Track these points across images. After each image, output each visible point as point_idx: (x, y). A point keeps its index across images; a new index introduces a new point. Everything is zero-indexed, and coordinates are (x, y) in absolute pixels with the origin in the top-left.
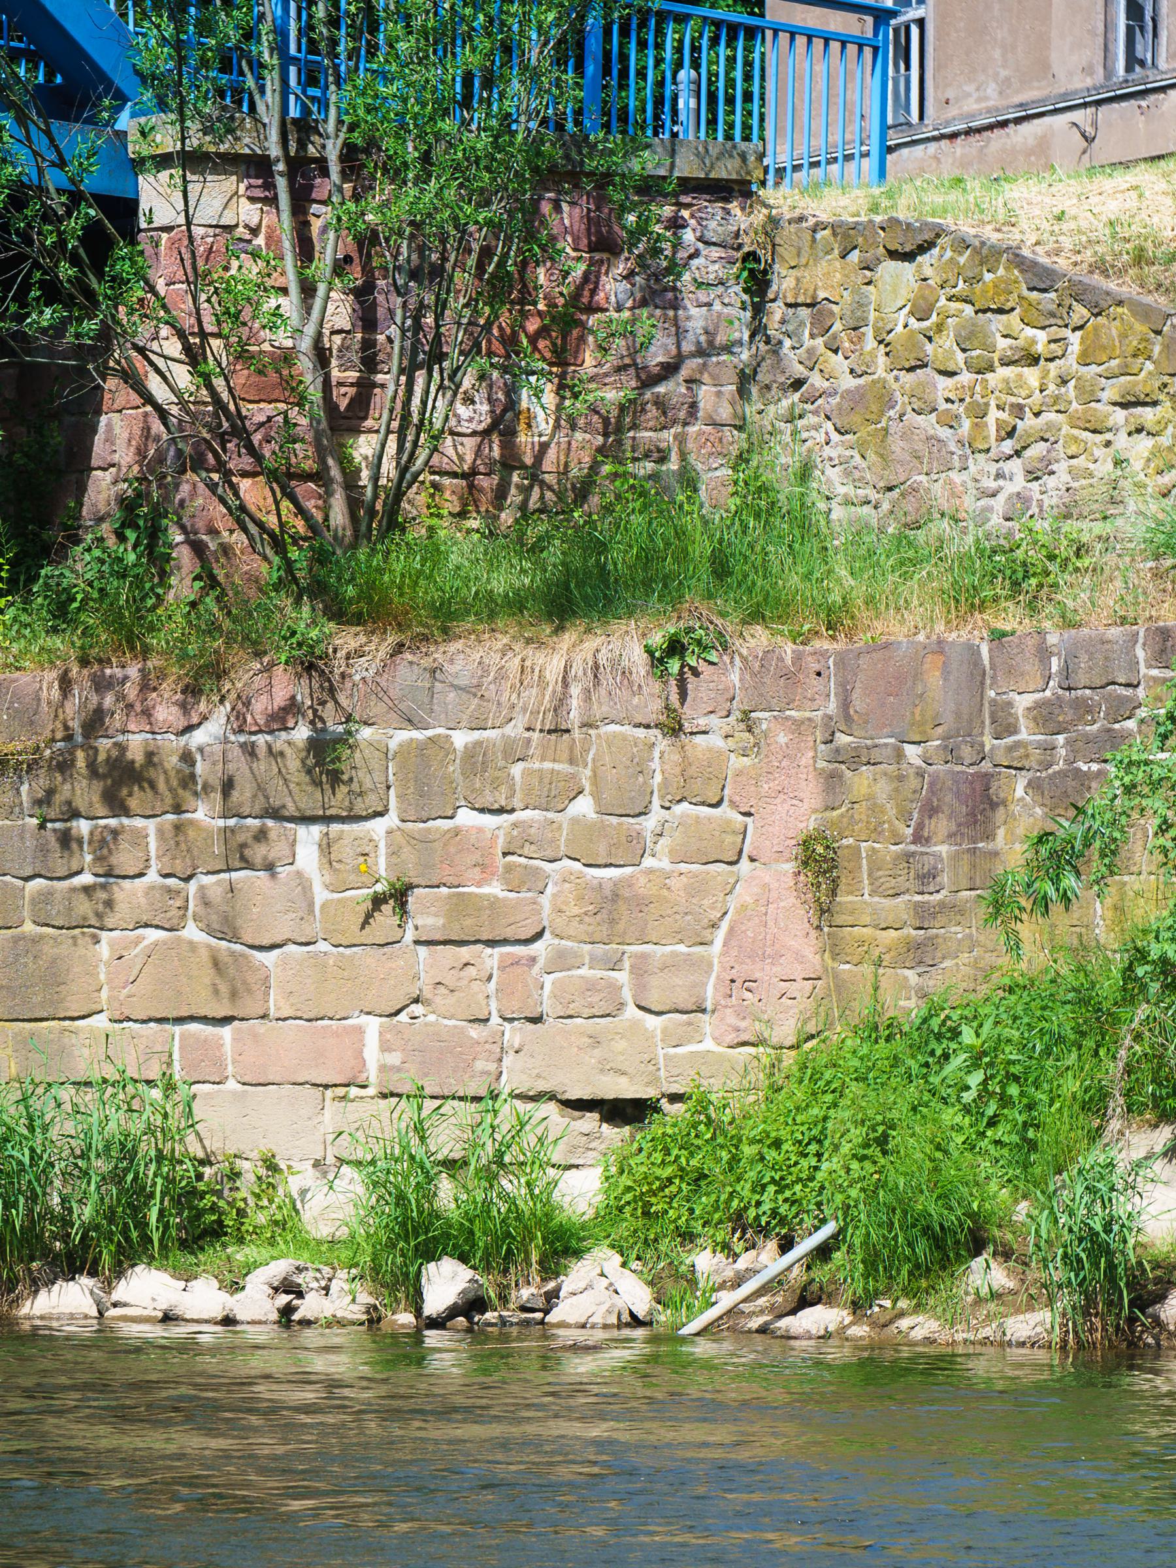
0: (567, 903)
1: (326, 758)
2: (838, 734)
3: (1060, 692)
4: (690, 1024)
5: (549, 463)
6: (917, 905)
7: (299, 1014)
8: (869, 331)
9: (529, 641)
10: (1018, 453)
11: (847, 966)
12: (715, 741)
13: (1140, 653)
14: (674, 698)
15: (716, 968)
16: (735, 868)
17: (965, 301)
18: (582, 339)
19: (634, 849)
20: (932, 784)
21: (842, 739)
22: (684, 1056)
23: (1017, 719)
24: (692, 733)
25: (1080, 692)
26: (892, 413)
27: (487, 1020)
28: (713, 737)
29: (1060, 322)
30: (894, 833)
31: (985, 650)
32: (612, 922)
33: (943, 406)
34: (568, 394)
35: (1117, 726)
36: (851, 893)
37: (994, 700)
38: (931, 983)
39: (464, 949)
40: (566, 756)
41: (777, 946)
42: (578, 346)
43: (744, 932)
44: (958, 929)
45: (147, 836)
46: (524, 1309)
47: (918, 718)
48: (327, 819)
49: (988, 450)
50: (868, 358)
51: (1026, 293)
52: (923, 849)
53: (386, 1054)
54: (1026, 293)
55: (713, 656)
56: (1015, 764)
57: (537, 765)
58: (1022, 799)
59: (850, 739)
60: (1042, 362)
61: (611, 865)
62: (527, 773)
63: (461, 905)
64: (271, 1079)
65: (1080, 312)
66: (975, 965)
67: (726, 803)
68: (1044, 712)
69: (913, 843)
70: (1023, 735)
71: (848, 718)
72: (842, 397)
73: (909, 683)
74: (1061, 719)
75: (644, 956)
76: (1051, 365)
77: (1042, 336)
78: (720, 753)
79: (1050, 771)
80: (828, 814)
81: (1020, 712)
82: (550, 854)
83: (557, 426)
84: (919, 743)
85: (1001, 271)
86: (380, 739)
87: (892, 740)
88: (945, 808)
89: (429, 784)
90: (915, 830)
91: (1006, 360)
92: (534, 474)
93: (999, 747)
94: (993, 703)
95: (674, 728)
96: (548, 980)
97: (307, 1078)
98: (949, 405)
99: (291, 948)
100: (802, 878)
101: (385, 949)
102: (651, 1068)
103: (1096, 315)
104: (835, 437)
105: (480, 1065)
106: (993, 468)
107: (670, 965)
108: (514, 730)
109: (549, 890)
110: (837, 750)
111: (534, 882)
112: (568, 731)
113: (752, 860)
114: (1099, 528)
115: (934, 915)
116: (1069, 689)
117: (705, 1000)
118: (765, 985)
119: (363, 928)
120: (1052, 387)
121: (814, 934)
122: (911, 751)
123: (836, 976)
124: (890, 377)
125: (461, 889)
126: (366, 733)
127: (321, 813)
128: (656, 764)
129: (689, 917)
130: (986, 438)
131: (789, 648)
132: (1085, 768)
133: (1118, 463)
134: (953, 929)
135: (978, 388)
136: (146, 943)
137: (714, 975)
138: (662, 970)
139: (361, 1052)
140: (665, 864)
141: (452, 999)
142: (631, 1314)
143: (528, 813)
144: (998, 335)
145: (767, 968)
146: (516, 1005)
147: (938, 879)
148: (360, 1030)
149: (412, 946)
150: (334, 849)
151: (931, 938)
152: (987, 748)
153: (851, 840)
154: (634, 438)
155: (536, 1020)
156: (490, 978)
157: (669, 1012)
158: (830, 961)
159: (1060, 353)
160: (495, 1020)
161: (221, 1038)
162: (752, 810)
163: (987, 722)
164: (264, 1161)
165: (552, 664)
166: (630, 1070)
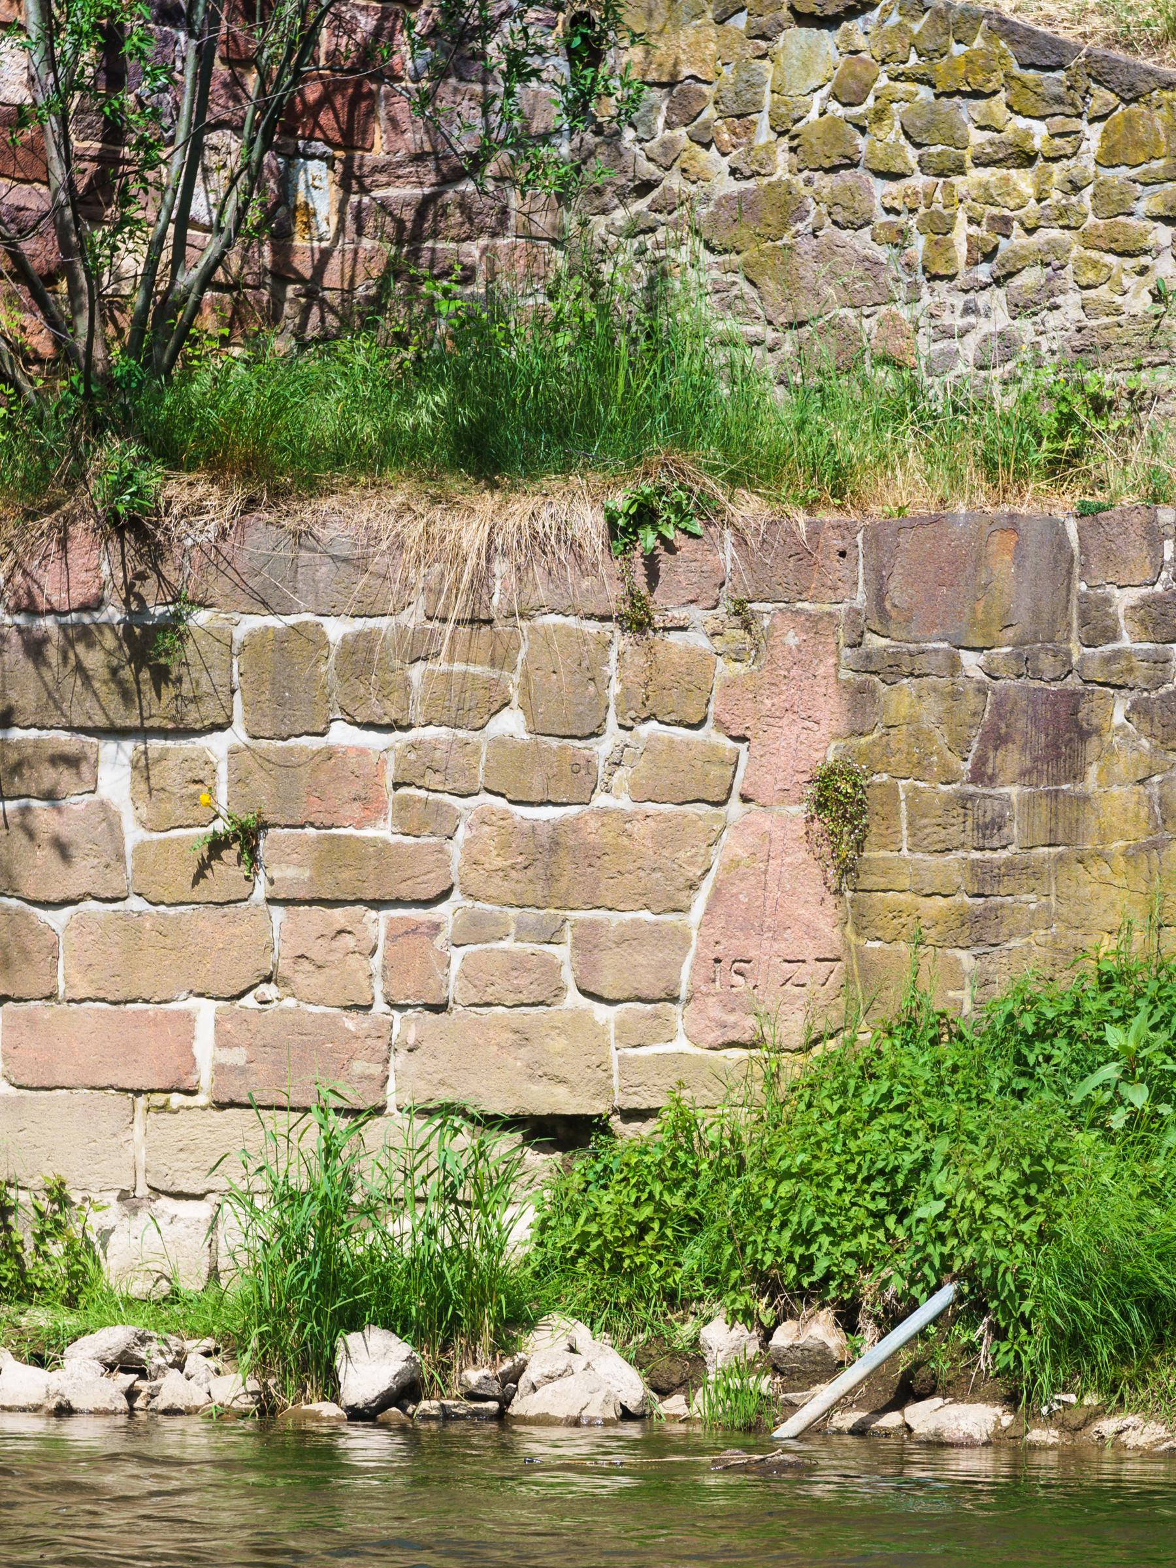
0: (486, 853)
1: (149, 649)
2: (868, 635)
4: (656, 1016)
5: (332, 277)
6: (975, 864)
7: (102, 994)
8: (763, 121)
9: (435, 500)
10: (998, 282)
11: (877, 944)
12: (697, 640)
14: (640, 580)
15: (694, 943)
16: (721, 811)
17: (920, 81)
18: (371, 112)
19: (580, 782)
20: (998, 705)
21: (875, 642)
22: (647, 1060)
23: (1118, 620)
24: (665, 629)
26: (800, 226)
27: (370, 1007)
28: (694, 634)
29: (1069, 110)
30: (946, 768)
31: (1072, 527)
32: (550, 879)
33: (882, 218)
34: (355, 187)
36: (884, 847)
37: (1085, 595)
38: (991, 968)
39: (338, 911)
40: (486, 655)
41: (781, 916)
42: (366, 123)
43: (735, 895)
47: (980, 616)
48: (142, 733)
49: (951, 278)
50: (762, 155)
51: (1016, 71)
52: (985, 791)
53: (225, 1050)
54: (1016, 71)
55: (697, 527)
56: (1114, 680)
58: (1121, 727)
59: (885, 642)
60: (1039, 162)
61: (549, 803)
62: (429, 677)
63: (335, 852)
65: (1101, 98)
66: (1054, 946)
67: (710, 723)
68: (1155, 613)
70: (1125, 642)
71: (883, 614)
72: (719, 205)
73: (970, 570)
75: (594, 925)
76: (1055, 167)
77: (1040, 129)
78: (704, 656)
79: (1162, 691)
80: (854, 741)
81: (1121, 612)
82: (462, 786)
83: (341, 229)
84: (980, 650)
85: (978, 42)
86: (225, 627)
87: (945, 645)
88: (1017, 737)
89: (288, 685)
90: (974, 765)
91: (984, 159)
92: (312, 290)
94: (1083, 598)
95: (638, 622)
96: (457, 955)
98: (892, 218)
99: (92, 905)
100: (817, 825)
101: (226, 909)
102: (601, 1074)
103: (1128, 102)
104: (706, 257)
105: (358, 1067)
106: (959, 301)
107: (629, 938)
108: (413, 618)
109: (462, 834)
110: (868, 657)
111: (439, 823)
112: (490, 621)
113: (745, 799)
114: (1128, 381)
115: (998, 879)
117: (678, 985)
118: (763, 967)
119: (195, 882)
120: (1056, 195)
121: (831, 900)
122: (970, 661)
123: (861, 955)
124: (798, 180)
125: (334, 831)
126: (201, 617)
127: (137, 723)
128: (612, 669)
129: (658, 875)
130: (950, 261)
131: (802, 518)
133: (1158, 297)
134: (1024, 897)
135: (938, 195)
138: (618, 944)
139: (190, 1046)
140: (624, 803)
141: (319, 979)
142: (623, 1407)
143: (431, 732)
144: (971, 126)
145: (766, 944)
146: (411, 986)
147: (1005, 830)
148: (188, 1018)
149: (264, 906)
152: (1075, 658)
153: (885, 777)
154: (433, 250)
155: (439, 1008)
156: (373, 952)
157: (628, 1000)
158: (853, 937)
159: (1069, 151)
160: (380, 1006)
162: (748, 734)
163: (1075, 624)
165: (470, 534)
166: (571, 1077)
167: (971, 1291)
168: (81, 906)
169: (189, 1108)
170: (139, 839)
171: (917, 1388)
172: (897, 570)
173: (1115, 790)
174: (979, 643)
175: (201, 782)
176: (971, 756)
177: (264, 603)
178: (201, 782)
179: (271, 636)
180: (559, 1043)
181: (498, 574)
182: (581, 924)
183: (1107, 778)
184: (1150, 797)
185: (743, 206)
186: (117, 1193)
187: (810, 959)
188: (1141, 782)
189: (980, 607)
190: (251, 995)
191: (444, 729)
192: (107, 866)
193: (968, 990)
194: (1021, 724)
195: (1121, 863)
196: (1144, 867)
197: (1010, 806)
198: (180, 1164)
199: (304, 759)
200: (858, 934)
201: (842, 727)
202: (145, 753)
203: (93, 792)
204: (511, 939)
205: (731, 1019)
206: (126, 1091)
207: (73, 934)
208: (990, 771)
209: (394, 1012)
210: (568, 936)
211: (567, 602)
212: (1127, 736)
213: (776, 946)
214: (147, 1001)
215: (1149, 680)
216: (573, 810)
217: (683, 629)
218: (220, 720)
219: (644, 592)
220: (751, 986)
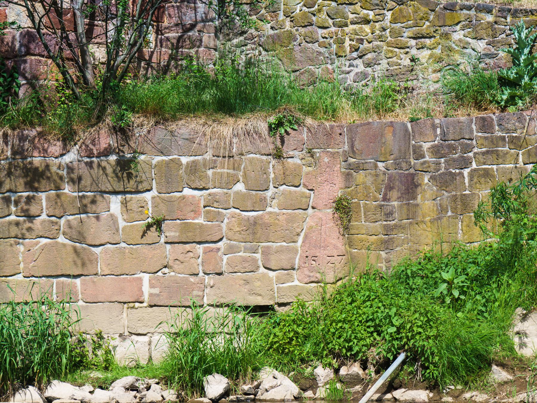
0: (234, 226)
1: (125, 166)
3: (441, 142)
4: (288, 274)
5: (154, 59)
6: (385, 225)
7: (113, 273)
8: (281, 13)
9: (214, 121)
10: (360, 57)
11: (356, 250)
12: (297, 161)
13: (474, 127)
14: (279, 143)
15: (299, 252)
16: (306, 212)
18: (164, 12)
19: (262, 204)
21: (352, 160)
22: (286, 288)
24: (288, 158)
25: (449, 142)
26: (295, 43)
27: (198, 274)
28: (295, 159)
29: (381, 8)
30: (375, 197)
31: (409, 125)
32: (254, 233)
33: (322, 40)
34: (160, 33)
35: (465, 155)
36: (357, 221)
37: (414, 145)
38: (391, 257)
39: (187, 245)
42: (162, 15)
43: (312, 237)
44: (402, 235)
45: (41, 200)
46: (246, 394)
47: (383, 152)
48: (124, 193)
50: (282, 23)
52: (387, 203)
53: (153, 289)
55: (296, 127)
56: (424, 170)
57: (219, 170)
58: (427, 184)
61: (253, 211)
62: (214, 174)
63: (187, 228)
64: (100, 300)
67: (302, 185)
68: (436, 150)
69: (383, 201)
70: (427, 158)
71: (354, 152)
72: (268, 37)
73: (379, 138)
74: (443, 152)
75: (268, 247)
76: (377, 24)
78: (299, 166)
79: (439, 173)
80: (346, 190)
81: (425, 150)
83: (156, 46)
84: (383, 162)
86: (149, 160)
87: (373, 160)
89: (169, 176)
90: (383, 196)
92: (149, 63)
93: (417, 163)
94: (414, 146)
95: (278, 156)
96: (225, 258)
97: (117, 300)
98: (325, 40)
99: (109, 246)
100: (336, 215)
101: (152, 246)
102: (271, 293)
103: (400, 5)
104: (263, 53)
105: (195, 293)
106: (348, 63)
107: (279, 251)
109: (226, 221)
110: (350, 165)
111: (219, 217)
113: (313, 208)
116: (445, 141)
117: (295, 265)
118: (321, 258)
119: (142, 237)
121: (341, 237)
123: (351, 254)
124: (294, 30)
125: (185, 221)
126: (142, 157)
128: (271, 170)
129: (287, 231)
132: (454, 171)
133: (413, 60)
134: (400, 235)
135: (339, 33)
136: (41, 244)
137: (299, 254)
138: (276, 253)
140: (276, 210)
141: (182, 266)
143: (215, 190)
144: (349, 13)
145: (322, 251)
146: (211, 268)
147: (394, 215)
148: (140, 279)
149: (164, 244)
150: (128, 204)
151: (391, 239)
152: (412, 164)
153: (356, 200)
154: (182, 52)
155: (220, 274)
156: (199, 258)
158: (348, 249)
160: (201, 274)
161: (76, 283)
162: (314, 188)
163: (412, 154)
164: (97, 335)
167: (411, 355)
168: (106, 246)
169: (141, 307)
170: (124, 225)
171: (395, 386)
172: (357, 139)
173: (426, 202)
174: (383, 160)
175: (143, 207)
176: (382, 193)
177: (162, 152)
178: (143, 207)
179: (164, 162)
180: (258, 284)
181: (235, 143)
182: (264, 247)
183: (424, 199)
184: (437, 204)
185: (275, 39)
186: (118, 335)
187: (336, 256)
188: (434, 200)
189: (383, 149)
190: (160, 272)
191: (219, 189)
192: (114, 234)
193: (384, 263)
194: (397, 183)
195: (429, 224)
196: (436, 225)
197: (395, 208)
198: (138, 325)
199: (176, 199)
200: (350, 248)
201: (342, 185)
202: (125, 199)
203: (109, 211)
204: (242, 252)
205: (312, 274)
206: (121, 302)
207: (103, 255)
208: (388, 198)
209: (206, 276)
210: (260, 251)
211: (257, 150)
212: (429, 186)
213: (325, 252)
214: (127, 275)
215: (435, 169)
216: (261, 212)
217: (292, 157)
218: (149, 188)
219: (280, 147)
220: (317, 264)
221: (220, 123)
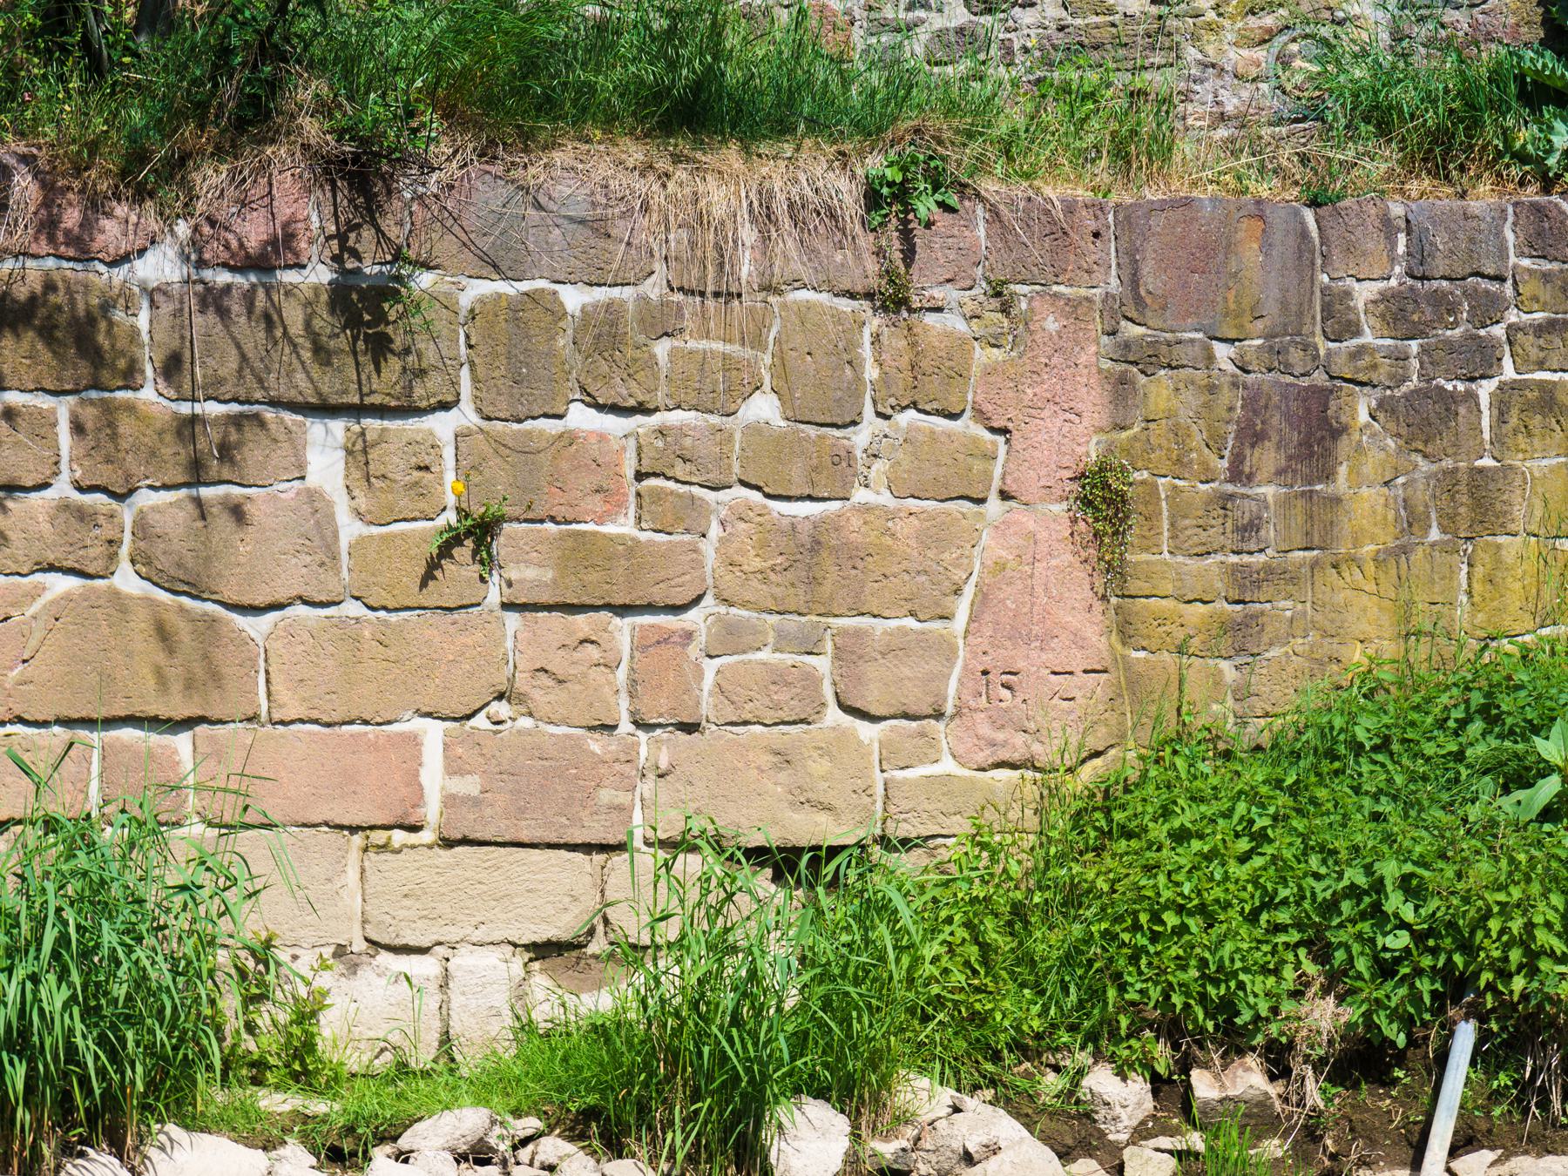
3: (1410, 281)
6: (1235, 569)
7: (315, 715)
9: (677, 159)
11: (1142, 654)
15: (961, 653)
19: (835, 474)
23: (1358, 315)
25: (1435, 284)
27: (615, 727)
28: (950, 318)
30: (1206, 467)
32: (813, 581)
35: (1482, 332)
37: (1328, 288)
39: (580, 619)
43: (1002, 601)
44: (1289, 604)
47: (1232, 306)
52: (1243, 490)
53: (456, 779)
56: (1362, 377)
57: (692, 344)
58: (1367, 426)
61: (810, 498)
62: (673, 354)
63: (582, 552)
68: (1394, 308)
69: (1231, 481)
70: (1368, 338)
74: (1415, 317)
75: (858, 634)
79: (1404, 389)
81: (1361, 306)
82: (714, 477)
84: (1231, 341)
86: (453, 289)
87: (1200, 335)
90: (1232, 463)
93: (1337, 352)
94: (1325, 290)
95: (893, 300)
97: (328, 816)
99: (300, 610)
101: (456, 616)
107: (896, 648)
108: (653, 289)
109: (715, 531)
110: (1127, 346)
111: (689, 517)
113: (1005, 496)
115: (1258, 584)
117: (945, 700)
119: (424, 584)
121: (1098, 606)
123: (1128, 665)
125: (574, 526)
126: (425, 280)
127: (356, 400)
128: (867, 351)
129: (924, 578)
132: (1449, 387)
134: (1282, 604)
136: (48, 596)
137: (960, 663)
139: (416, 774)
140: (885, 499)
141: (559, 694)
145: (1034, 654)
146: (664, 703)
147: (1263, 533)
148: (414, 741)
150: (373, 454)
151: (1254, 617)
152: (1322, 352)
153: (1146, 474)
155: (690, 728)
158: (1119, 647)
160: (626, 727)
162: (1010, 426)
163: (1319, 318)
165: (718, 197)
172: (1150, 254)
173: (1365, 491)
174: (1232, 334)
175: (427, 468)
176: (1227, 453)
177: (495, 266)
178: (427, 468)
179: (504, 304)
180: (820, 766)
181: (748, 244)
183: (1357, 479)
184: (1396, 497)
187: (1078, 671)
188: (1386, 483)
189: (1231, 296)
191: (693, 413)
194: (1275, 421)
195: (1370, 568)
196: (1394, 572)
197: (1267, 508)
199: (544, 444)
200: (1124, 644)
201: (1105, 422)
202: (363, 434)
204: (768, 649)
205: (1000, 736)
208: (1247, 470)
209: (640, 733)
210: (829, 646)
212: (1373, 435)
213: (1044, 657)
215: (1392, 377)
217: (939, 310)
218: (450, 398)
219: (902, 270)
220: (1019, 700)
221: (699, 170)
